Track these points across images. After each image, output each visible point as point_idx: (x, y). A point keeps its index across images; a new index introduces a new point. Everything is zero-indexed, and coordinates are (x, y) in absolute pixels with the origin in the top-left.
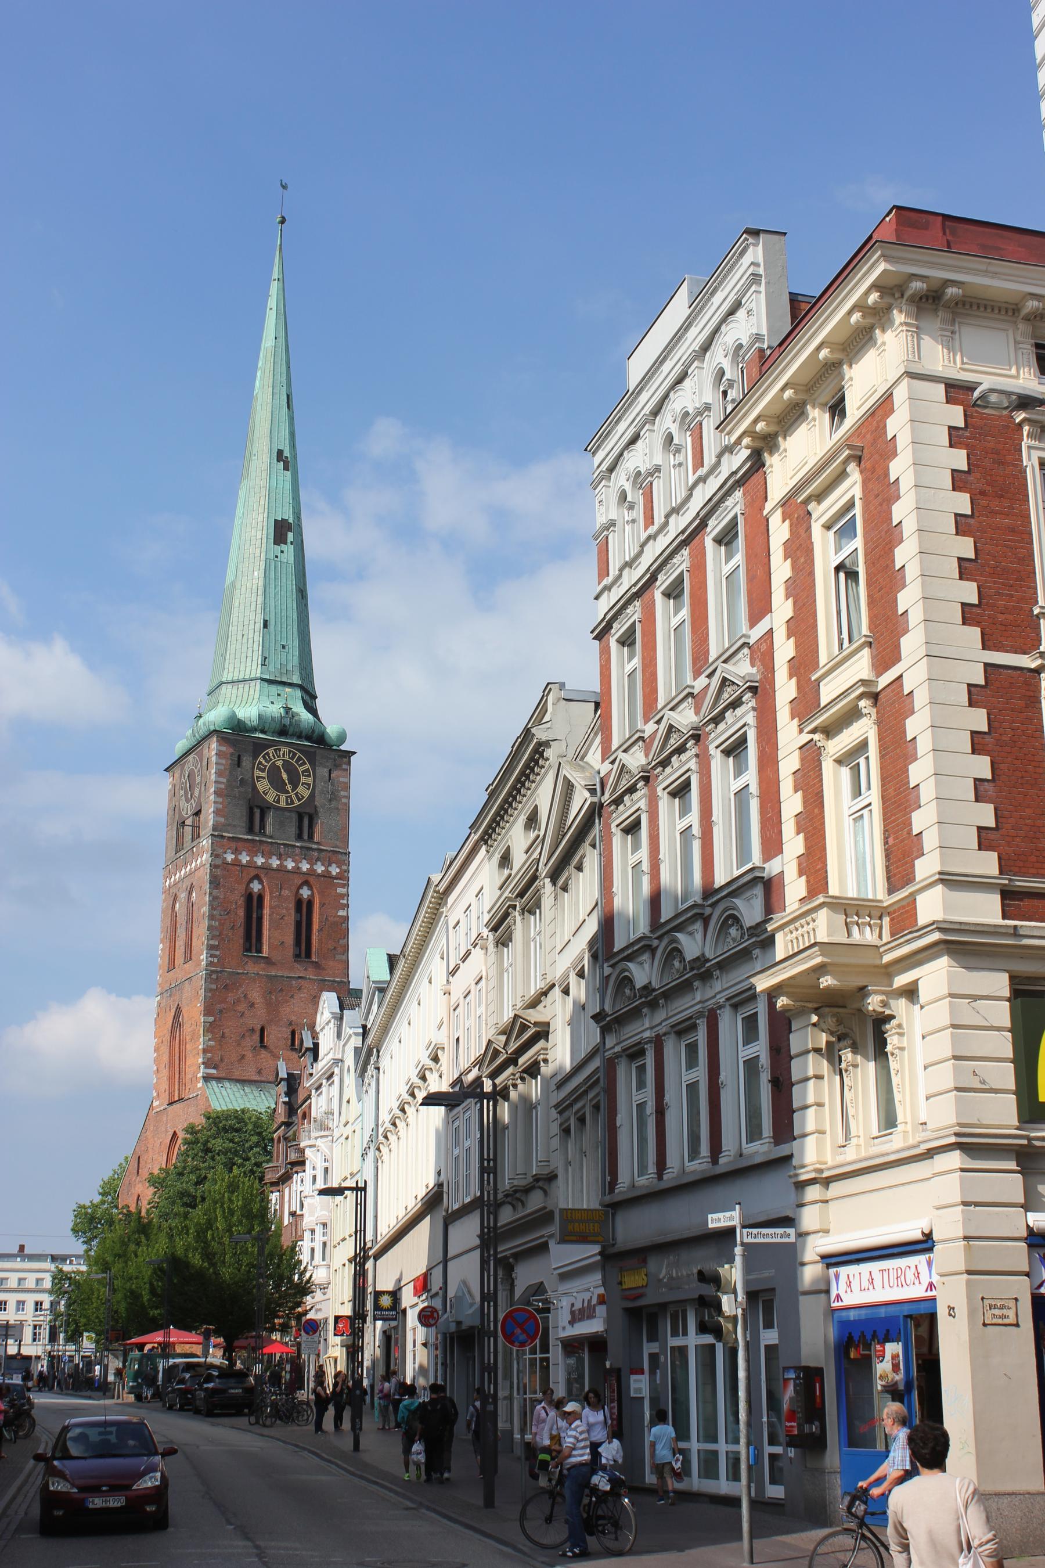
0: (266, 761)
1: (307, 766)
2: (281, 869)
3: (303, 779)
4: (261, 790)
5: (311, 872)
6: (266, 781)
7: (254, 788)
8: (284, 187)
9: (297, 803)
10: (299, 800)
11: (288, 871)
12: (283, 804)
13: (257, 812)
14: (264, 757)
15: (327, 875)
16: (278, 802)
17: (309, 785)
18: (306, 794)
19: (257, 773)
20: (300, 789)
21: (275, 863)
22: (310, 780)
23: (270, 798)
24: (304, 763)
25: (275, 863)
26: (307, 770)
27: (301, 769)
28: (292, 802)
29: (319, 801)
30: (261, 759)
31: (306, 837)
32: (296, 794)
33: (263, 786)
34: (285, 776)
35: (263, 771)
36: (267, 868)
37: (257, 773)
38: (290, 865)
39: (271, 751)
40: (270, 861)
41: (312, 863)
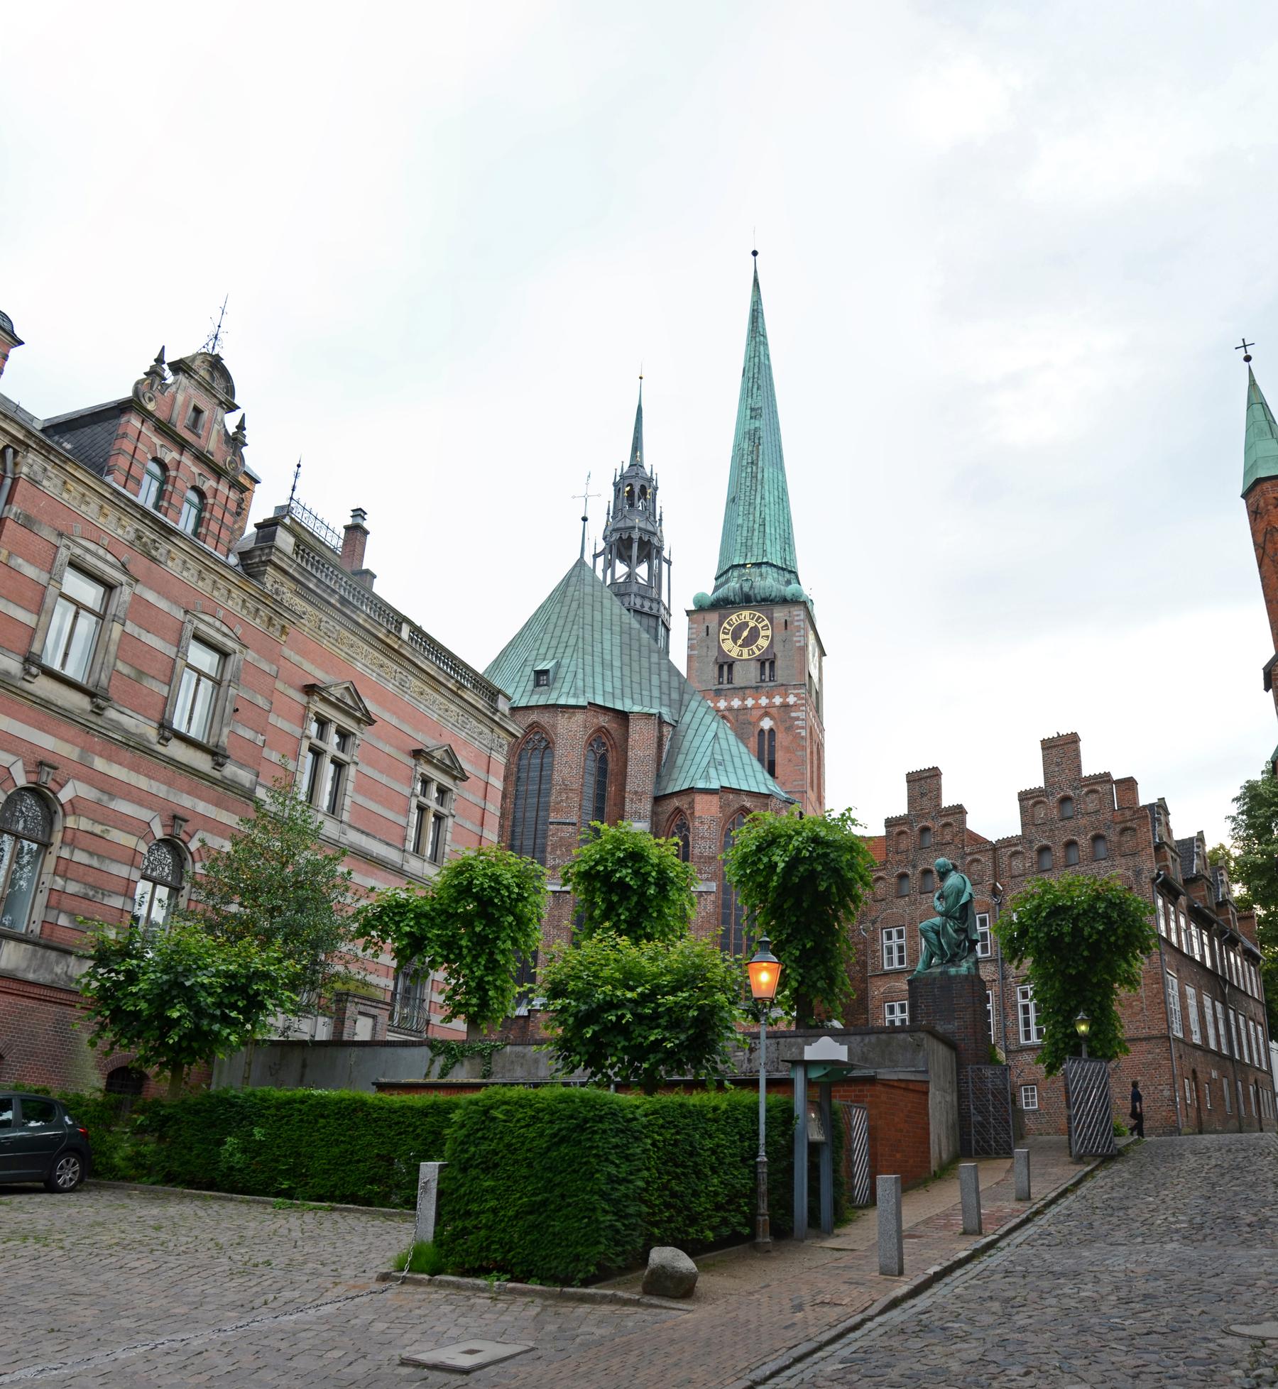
1: (766, 622)
3: (762, 633)
7: (720, 647)
8: (755, 253)
9: (757, 653)
12: (745, 656)
13: (725, 668)
15: (785, 706)
19: (722, 636)
22: (769, 633)
23: (734, 654)
27: (760, 626)
29: (778, 649)
30: (725, 625)
33: (728, 646)
34: (745, 634)
36: (730, 709)
37: (722, 636)
38: (750, 702)
39: (734, 617)
41: (770, 696)
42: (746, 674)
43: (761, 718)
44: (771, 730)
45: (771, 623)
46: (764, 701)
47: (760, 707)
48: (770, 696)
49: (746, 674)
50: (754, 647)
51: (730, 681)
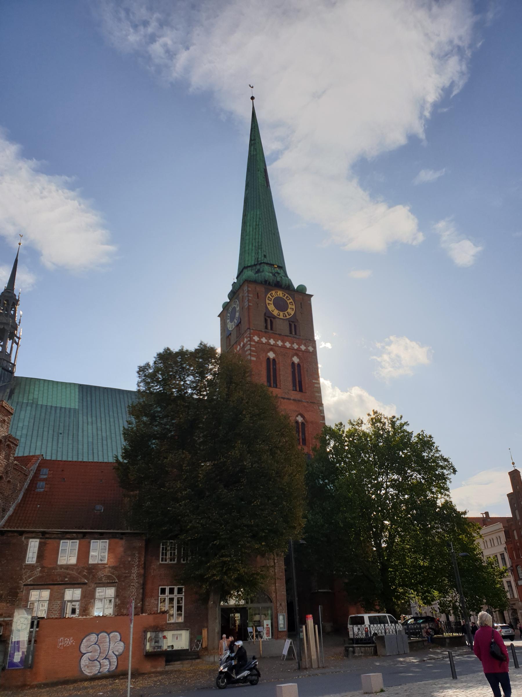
0: (272, 297)
1: (291, 300)
2: (284, 347)
3: (290, 306)
4: (270, 309)
5: (299, 350)
6: (272, 305)
7: (267, 308)
9: (288, 317)
10: (289, 315)
11: (287, 348)
12: (281, 317)
14: (270, 294)
16: (279, 315)
17: (293, 309)
18: (292, 313)
20: (289, 310)
21: (280, 343)
22: (294, 307)
24: (290, 299)
25: (280, 343)
26: (292, 302)
27: (288, 302)
28: (286, 316)
30: (269, 295)
31: (294, 333)
32: (287, 313)
33: (271, 307)
35: (271, 301)
36: (276, 345)
37: (267, 301)
38: (288, 345)
39: (274, 292)
40: (278, 343)
41: (299, 345)
42: (282, 327)
43: (293, 356)
44: (299, 364)
45: (294, 300)
46: (296, 346)
47: (293, 349)
48: (299, 345)
49: (282, 327)
50: (286, 313)
51: (272, 329)
